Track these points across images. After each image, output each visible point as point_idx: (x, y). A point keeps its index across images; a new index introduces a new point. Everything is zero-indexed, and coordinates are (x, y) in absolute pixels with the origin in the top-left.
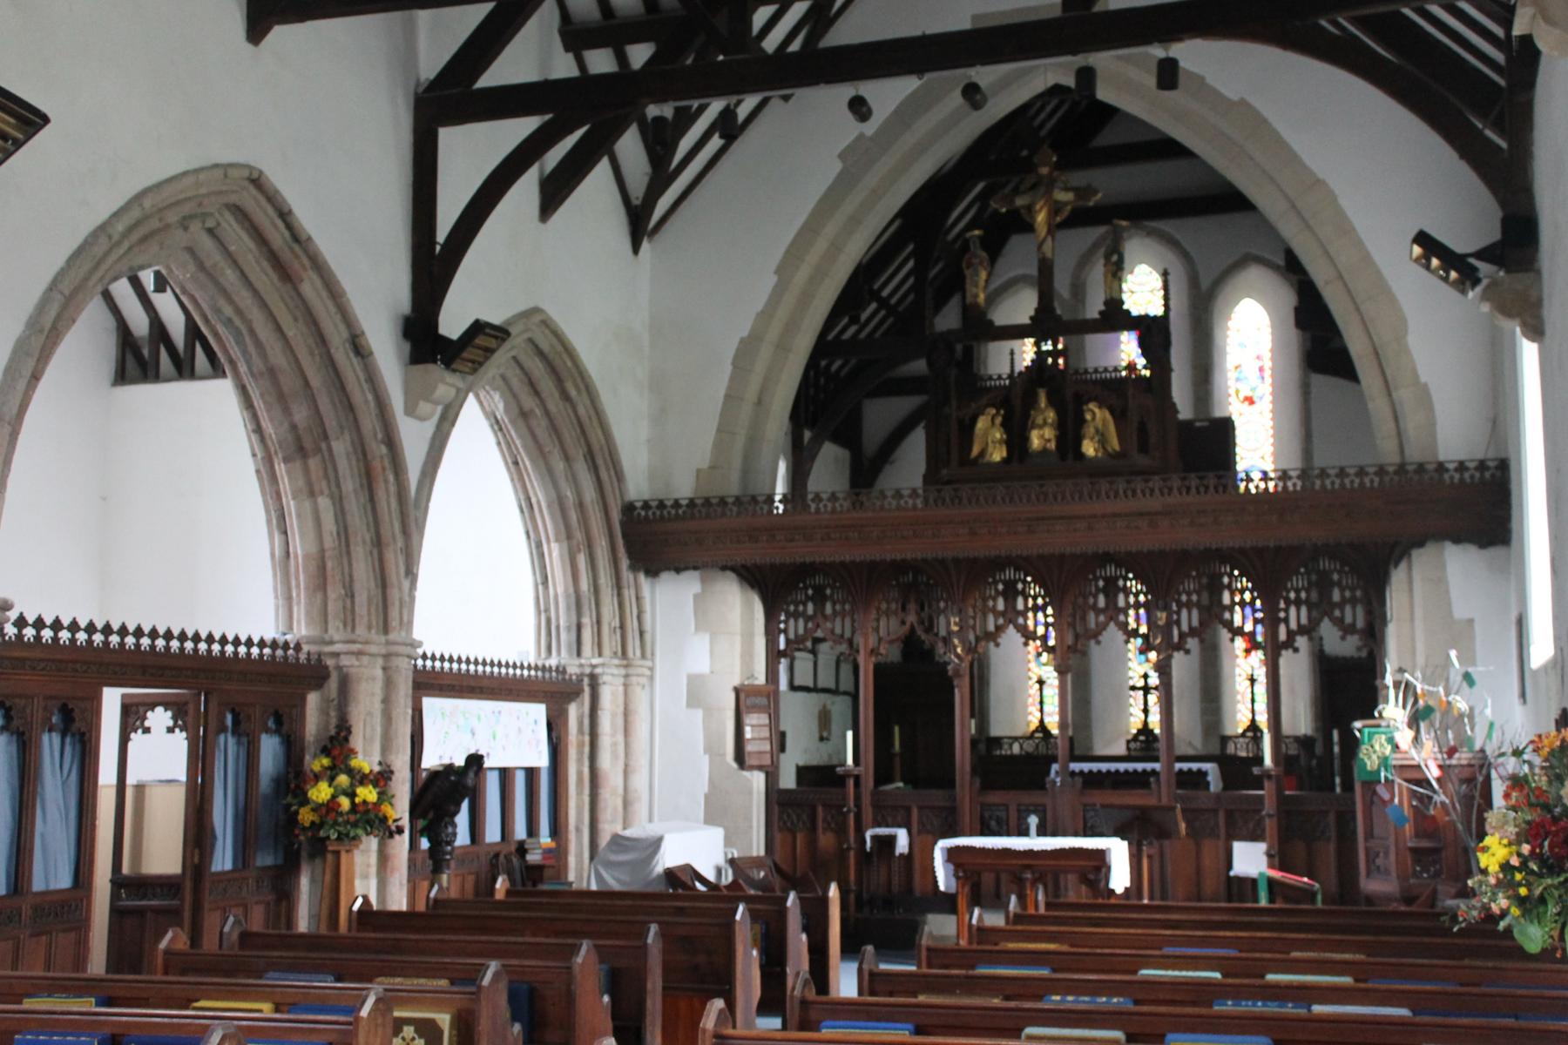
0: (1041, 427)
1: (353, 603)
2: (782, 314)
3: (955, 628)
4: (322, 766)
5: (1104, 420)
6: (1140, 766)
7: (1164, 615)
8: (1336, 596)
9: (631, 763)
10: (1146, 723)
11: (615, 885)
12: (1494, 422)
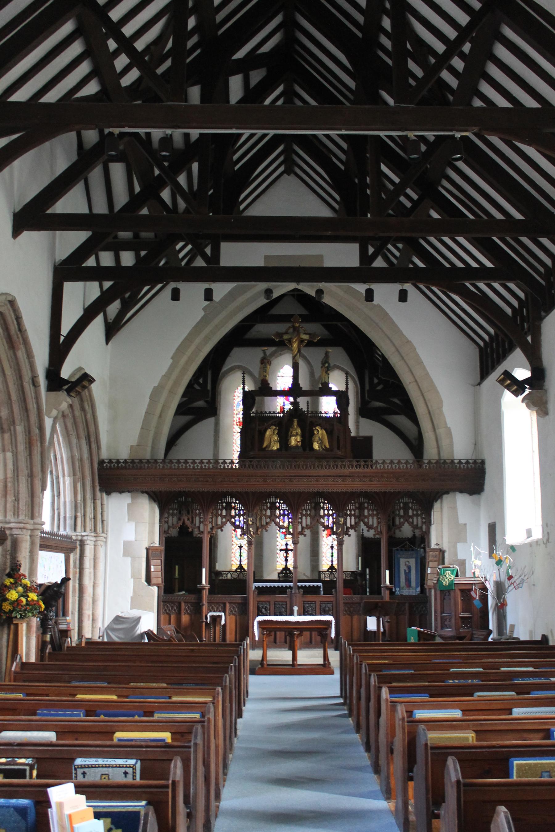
0: (296, 436)
1: (18, 504)
2: (174, 376)
3: (251, 523)
4: (11, 583)
5: (322, 434)
6: (284, 584)
7: (342, 519)
8: (366, 513)
9: (97, 582)
10: (286, 566)
11: (117, 640)
12: (475, 445)
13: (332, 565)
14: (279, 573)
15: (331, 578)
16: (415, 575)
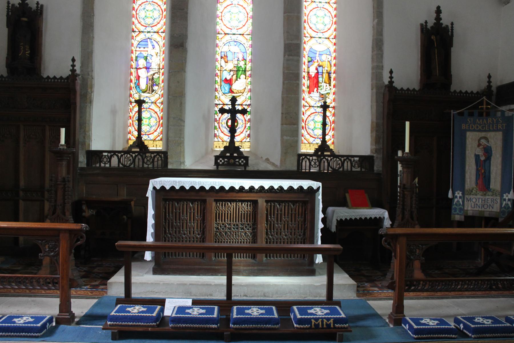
6: (227, 183)
13: (324, 141)
14: (217, 158)
15: (322, 169)
16: (500, 167)
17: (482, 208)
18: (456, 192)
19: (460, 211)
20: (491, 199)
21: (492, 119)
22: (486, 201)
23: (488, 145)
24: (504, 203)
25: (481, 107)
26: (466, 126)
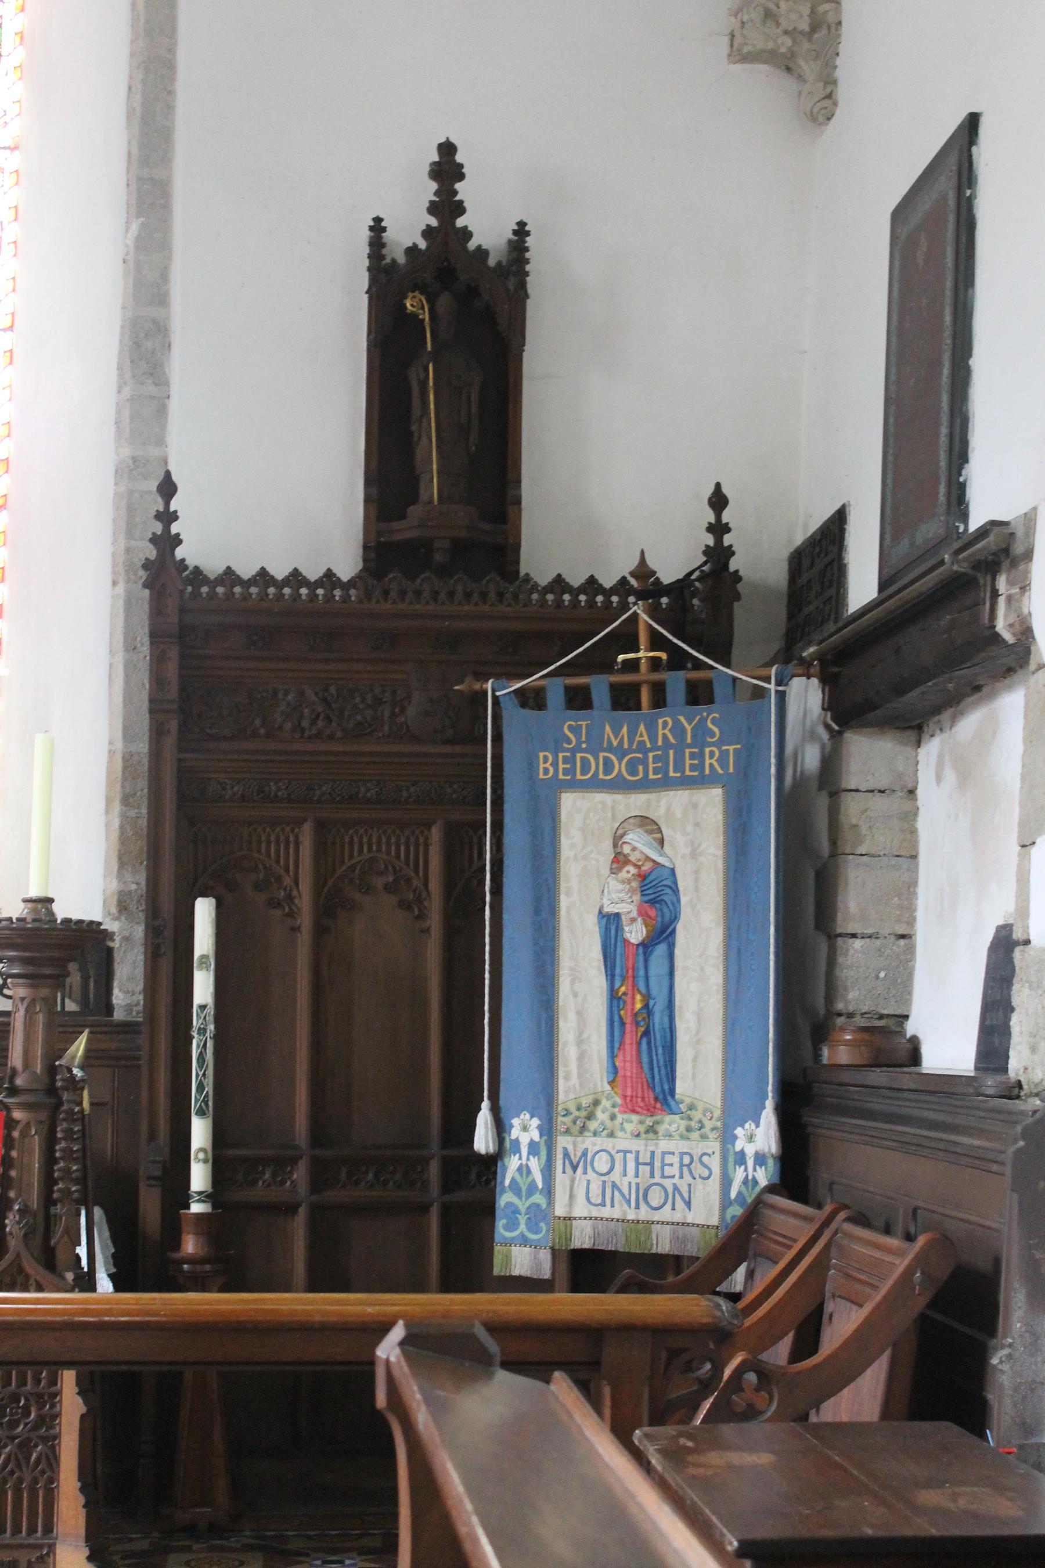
16: (716, 977)
17: (637, 1207)
18: (515, 1122)
19: (534, 1228)
20: (682, 1154)
21: (676, 722)
22: (657, 1164)
23: (660, 860)
24: (739, 1175)
25: (624, 661)
26: (555, 764)
